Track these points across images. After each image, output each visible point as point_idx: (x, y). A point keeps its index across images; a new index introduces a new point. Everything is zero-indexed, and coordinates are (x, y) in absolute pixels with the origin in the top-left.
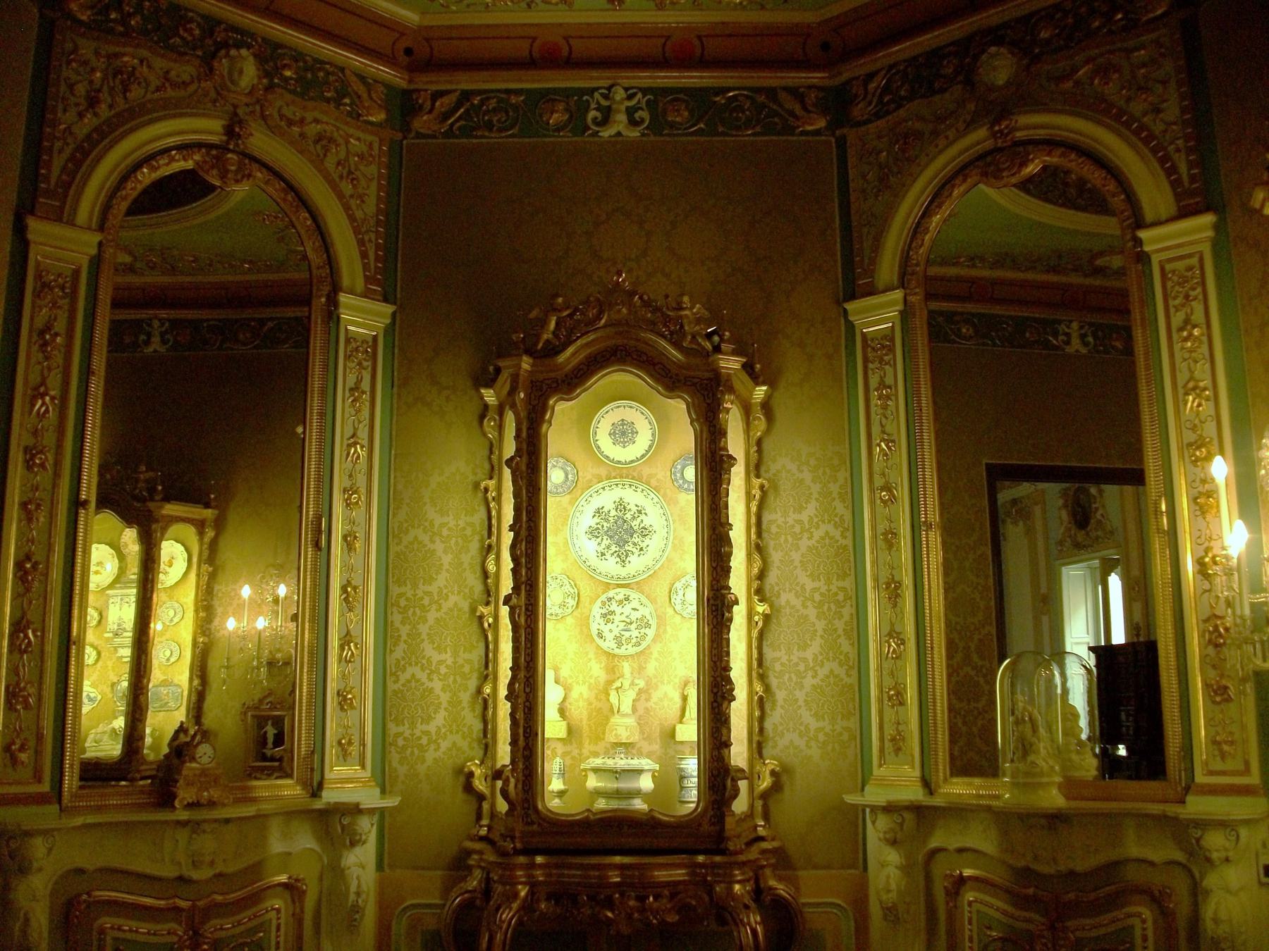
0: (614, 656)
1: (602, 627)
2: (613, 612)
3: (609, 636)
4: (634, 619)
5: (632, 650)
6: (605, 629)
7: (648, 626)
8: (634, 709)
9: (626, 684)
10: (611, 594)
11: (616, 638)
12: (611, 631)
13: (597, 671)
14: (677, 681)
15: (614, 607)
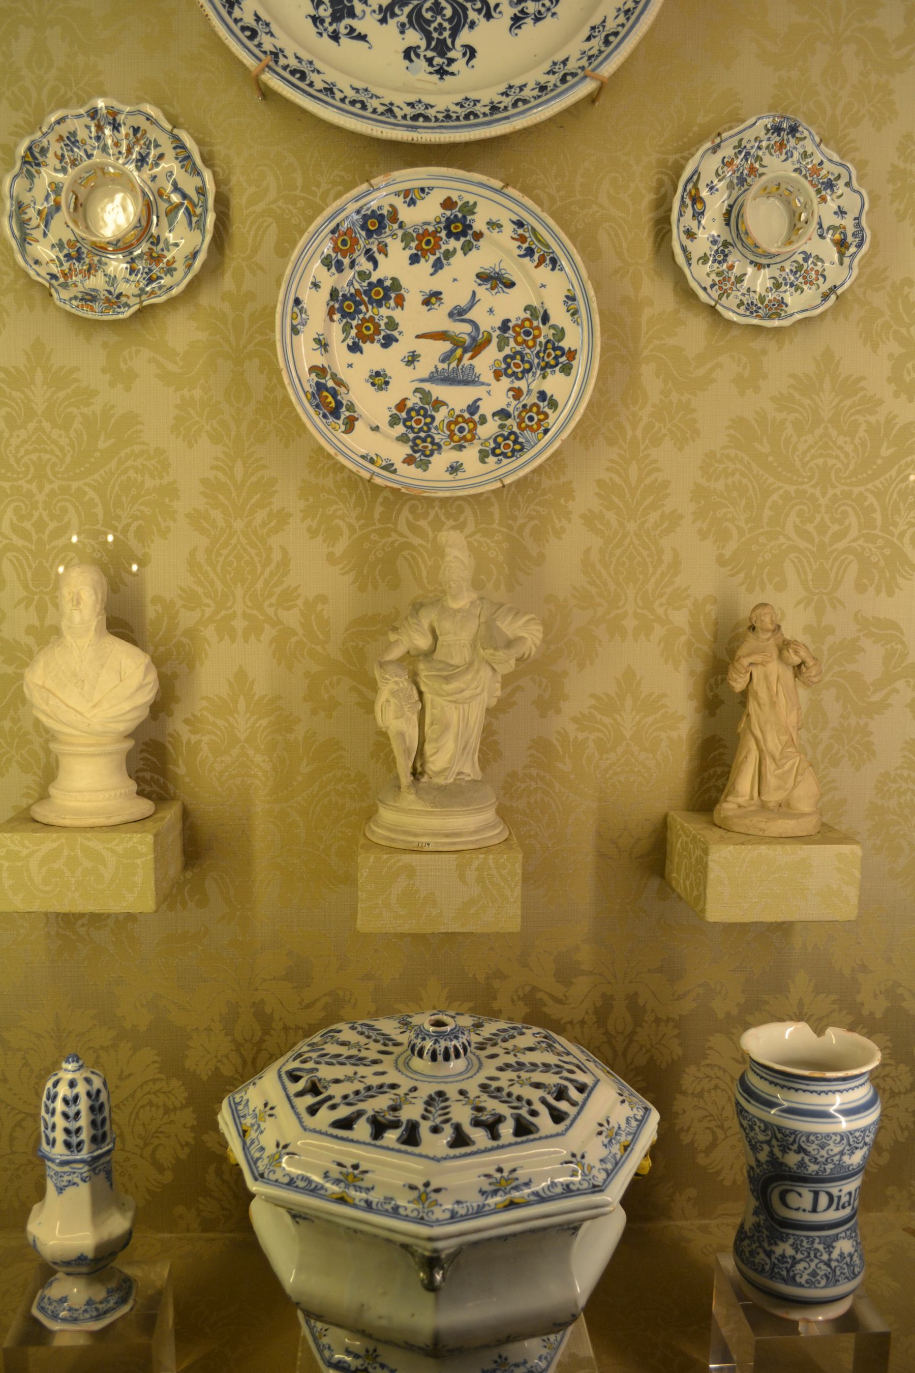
0: (398, 497)
1: (340, 357)
2: (390, 292)
3: (373, 406)
4: (488, 323)
5: (474, 469)
6: (353, 370)
7: (560, 358)
8: (489, 749)
9: (458, 641)
10: (381, 195)
11: (403, 414)
12: (379, 380)
13: (316, 569)
14: (680, 618)
15: (394, 263)
